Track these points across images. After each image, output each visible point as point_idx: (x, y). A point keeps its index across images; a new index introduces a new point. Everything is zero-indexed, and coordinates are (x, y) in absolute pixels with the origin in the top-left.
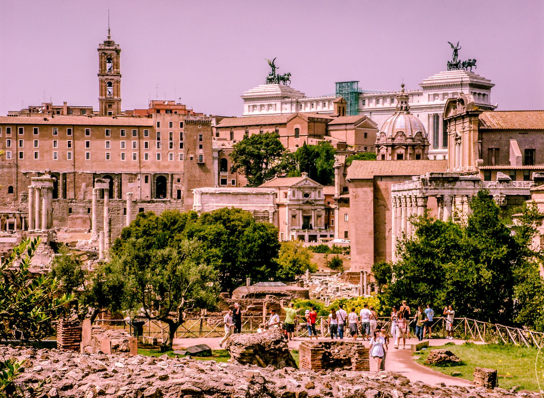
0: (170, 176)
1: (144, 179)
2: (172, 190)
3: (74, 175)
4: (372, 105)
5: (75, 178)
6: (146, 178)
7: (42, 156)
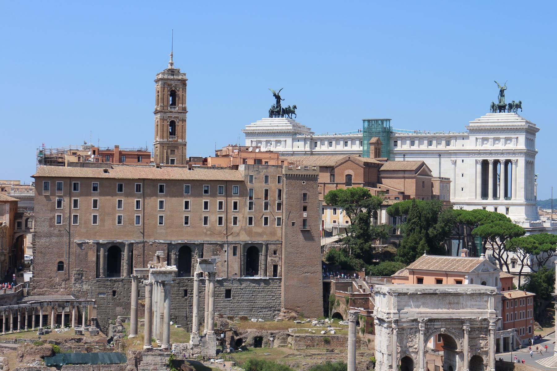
0: (264, 247)
1: (232, 251)
2: (266, 265)
3: (144, 246)
4: (406, 147)
5: (144, 251)
6: (235, 249)
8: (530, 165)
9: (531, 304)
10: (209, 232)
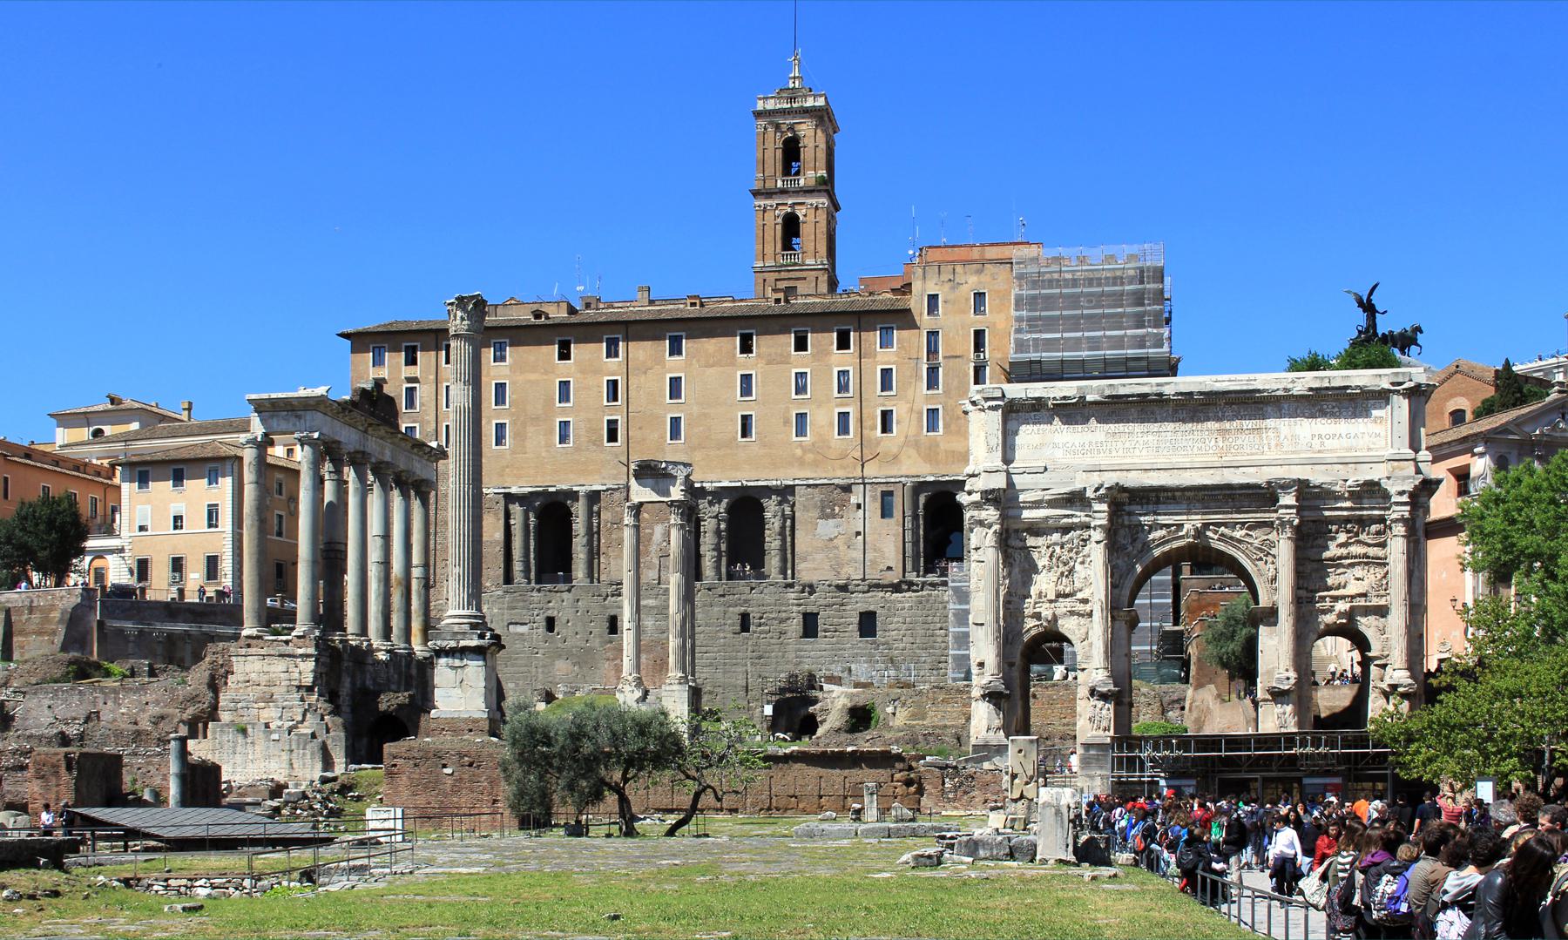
1: (878, 505)
6: (887, 496)
10: (810, 457)
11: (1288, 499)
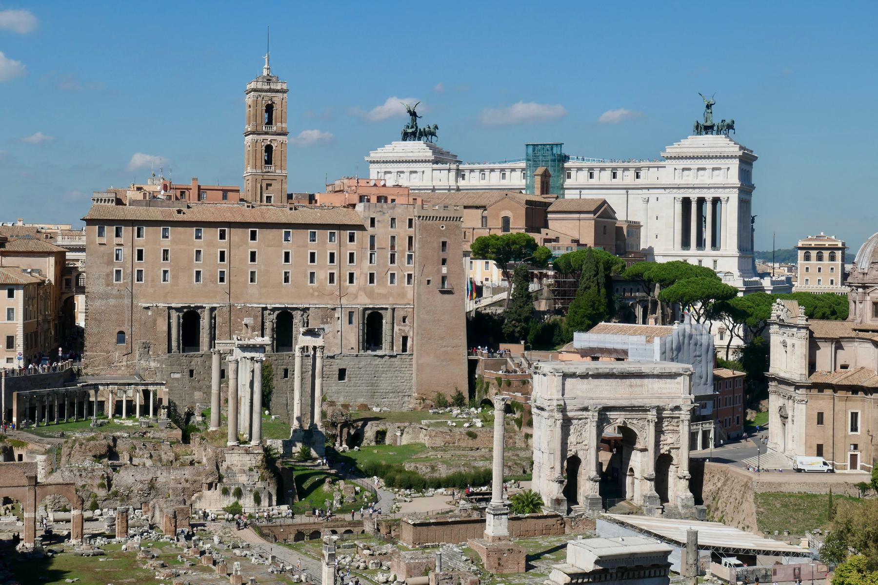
6: (351, 314)
7: (175, 277)
8: (744, 204)
9: (740, 387)
10: (316, 294)
11: (654, 412)
